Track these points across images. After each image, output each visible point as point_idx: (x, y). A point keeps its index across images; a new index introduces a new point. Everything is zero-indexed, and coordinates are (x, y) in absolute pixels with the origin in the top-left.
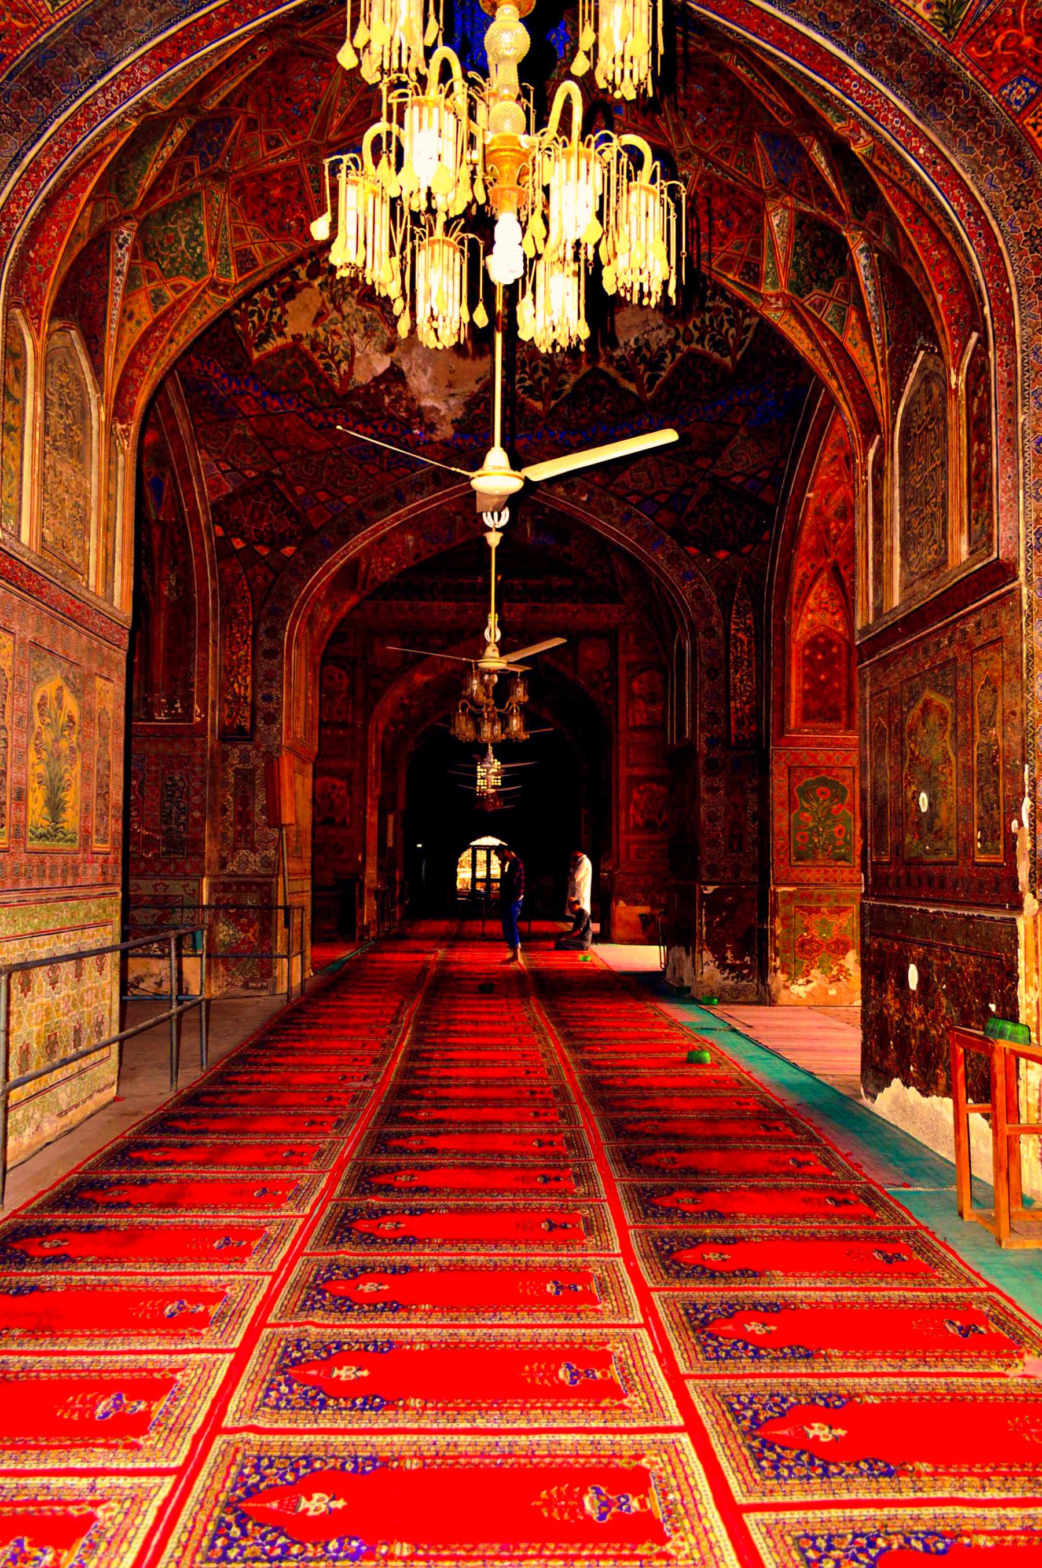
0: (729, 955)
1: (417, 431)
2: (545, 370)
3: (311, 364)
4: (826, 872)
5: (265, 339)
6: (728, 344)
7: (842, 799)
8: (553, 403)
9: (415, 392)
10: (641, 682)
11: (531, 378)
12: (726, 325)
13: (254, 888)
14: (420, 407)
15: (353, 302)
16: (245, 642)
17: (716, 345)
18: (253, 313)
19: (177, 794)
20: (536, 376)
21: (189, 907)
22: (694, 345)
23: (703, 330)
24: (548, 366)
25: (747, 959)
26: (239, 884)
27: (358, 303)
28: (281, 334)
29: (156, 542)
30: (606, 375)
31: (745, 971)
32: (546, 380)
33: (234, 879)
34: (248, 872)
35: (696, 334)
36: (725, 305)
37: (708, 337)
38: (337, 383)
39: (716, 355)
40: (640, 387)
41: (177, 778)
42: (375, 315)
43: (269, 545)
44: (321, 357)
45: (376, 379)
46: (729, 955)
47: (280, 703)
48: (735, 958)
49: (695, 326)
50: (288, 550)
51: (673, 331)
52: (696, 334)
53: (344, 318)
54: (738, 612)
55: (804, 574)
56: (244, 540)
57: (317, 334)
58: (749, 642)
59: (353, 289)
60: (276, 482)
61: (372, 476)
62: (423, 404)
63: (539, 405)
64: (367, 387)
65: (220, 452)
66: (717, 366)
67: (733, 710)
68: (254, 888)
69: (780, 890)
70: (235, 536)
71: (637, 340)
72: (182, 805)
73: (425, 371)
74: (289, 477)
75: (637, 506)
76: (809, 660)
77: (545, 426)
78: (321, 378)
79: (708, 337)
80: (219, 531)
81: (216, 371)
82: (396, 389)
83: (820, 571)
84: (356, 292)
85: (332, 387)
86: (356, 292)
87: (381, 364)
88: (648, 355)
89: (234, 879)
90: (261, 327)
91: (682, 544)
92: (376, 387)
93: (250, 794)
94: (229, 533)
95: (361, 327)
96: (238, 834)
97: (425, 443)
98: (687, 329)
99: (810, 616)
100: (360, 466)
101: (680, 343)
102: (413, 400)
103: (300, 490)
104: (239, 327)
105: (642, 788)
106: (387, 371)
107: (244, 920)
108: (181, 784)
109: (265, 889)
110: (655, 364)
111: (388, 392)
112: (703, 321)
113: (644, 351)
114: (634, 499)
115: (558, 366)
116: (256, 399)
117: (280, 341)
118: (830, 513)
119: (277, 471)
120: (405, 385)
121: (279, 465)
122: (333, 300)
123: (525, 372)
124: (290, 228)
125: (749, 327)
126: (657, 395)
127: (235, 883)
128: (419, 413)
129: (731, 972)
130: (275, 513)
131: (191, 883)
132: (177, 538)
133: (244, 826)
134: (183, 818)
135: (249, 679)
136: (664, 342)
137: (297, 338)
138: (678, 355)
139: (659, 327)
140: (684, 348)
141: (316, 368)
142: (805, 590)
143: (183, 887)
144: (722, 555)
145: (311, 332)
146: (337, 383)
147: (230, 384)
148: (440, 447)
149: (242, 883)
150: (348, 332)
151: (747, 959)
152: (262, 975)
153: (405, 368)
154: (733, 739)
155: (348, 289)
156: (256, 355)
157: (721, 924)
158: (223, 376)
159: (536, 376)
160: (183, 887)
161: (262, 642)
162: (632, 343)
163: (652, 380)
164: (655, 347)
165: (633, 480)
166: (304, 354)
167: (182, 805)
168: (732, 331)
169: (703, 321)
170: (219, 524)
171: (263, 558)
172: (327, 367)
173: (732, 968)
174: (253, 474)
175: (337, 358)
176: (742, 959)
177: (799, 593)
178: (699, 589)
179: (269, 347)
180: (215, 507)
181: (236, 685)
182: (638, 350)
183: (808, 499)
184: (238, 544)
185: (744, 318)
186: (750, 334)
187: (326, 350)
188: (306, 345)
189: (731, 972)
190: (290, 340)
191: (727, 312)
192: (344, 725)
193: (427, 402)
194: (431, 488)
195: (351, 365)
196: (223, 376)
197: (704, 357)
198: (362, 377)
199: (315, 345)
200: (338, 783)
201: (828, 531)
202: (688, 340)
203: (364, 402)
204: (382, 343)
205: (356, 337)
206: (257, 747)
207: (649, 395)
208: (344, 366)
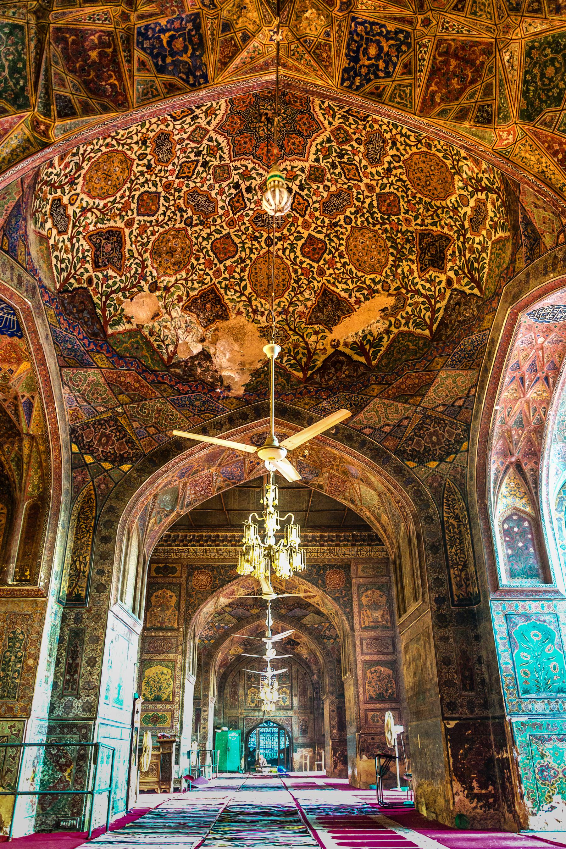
0: (475, 784)
1: (219, 390)
2: (303, 354)
3: (148, 344)
4: (549, 703)
5: (118, 323)
6: (426, 322)
7: (552, 641)
8: (310, 373)
9: (218, 367)
10: (367, 596)
11: (295, 358)
12: (424, 311)
13: (75, 730)
14: (221, 376)
15: (179, 310)
16: (88, 531)
17: (417, 325)
18: (110, 305)
19: (18, 645)
20: (298, 358)
21: (12, 746)
22: (402, 328)
23: (408, 319)
24: (306, 351)
25: (491, 788)
26: (62, 727)
27: (182, 311)
28: (129, 322)
29: (26, 451)
30: (344, 354)
31: (491, 800)
32: (305, 360)
33: (59, 723)
34: (71, 716)
35: (403, 321)
36: (421, 299)
37: (411, 321)
38: (165, 357)
39: (419, 331)
40: (367, 358)
41: (18, 632)
42: (193, 320)
43: (112, 462)
44: (156, 340)
45: (191, 357)
46: (475, 784)
47: (110, 576)
48: (481, 787)
49: (402, 317)
50: (126, 467)
51: (387, 322)
52: (403, 321)
53: (172, 319)
54: (449, 505)
55: (496, 469)
56: (95, 458)
57: (153, 326)
58: (459, 526)
59: (179, 302)
60: (119, 418)
61: (187, 418)
62: (223, 374)
63: (300, 375)
64: (186, 362)
65: (79, 391)
66: (420, 337)
67: (453, 576)
68: (75, 730)
69: (514, 720)
70: (86, 454)
71: (363, 331)
72: (19, 654)
73: (225, 355)
74: (129, 413)
75: (369, 436)
76: (507, 533)
77: (305, 387)
78: (155, 353)
79: (411, 321)
80: (75, 448)
81: (79, 333)
82: (205, 364)
83: (508, 468)
84: (181, 304)
85: (162, 359)
86: (181, 304)
87: (196, 349)
88: (371, 339)
89: (59, 723)
90: (115, 315)
91: (403, 460)
92: (192, 362)
93: (79, 648)
94: (83, 451)
95: (184, 326)
96: (67, 682)
97: (224, 398)
98: (396, 319)
99: (504, 500)
100: (179, 411)
101: (392, 328)
102: (216, 371)
103: (136, 424)
104: (99, 311)
105: (373, 669)
106: (200, 353)
107: (63, 760)
108: (21, 637)
109: (84, 731)
110: (376, 343)
111: (200, 365)
112: (407, 313)
113: (369, 337)
114: (367, 431)
115: (312, 351)
116: (107, 358)
117: (127, 326)
118: (511, 422)
119: (119, 409)
120: (211, 362)
121: (121, 405)
122: (165, 307)
123: (290, 355)
124: (105, 91)
125: (440, 308)
126: (380, 361)
127: (59, 726)
128: (221, 379)
129: (479, 801)
130: (118, 440)
131: (17, 724)
132: (42, 448)
133: (73, 675)
134: (19, 665)
135: (88, 558)
136: (382, 329)
137: (140, 327)
138: (392, 336)
139: (378, 321)
140: (396, 331)
141: (152, 346)
142: (499, 482)
143: (10, 727)
144: (433, 464)
145: (150, 324)
146: (165, 357)
147: (89, 345)
148: (234, 400)
149: (67, 726)
150: (175, 328)
151: (491, 788)
152: (73, 814)
153: (212, 351)
154: (456, 598)
155: (176, 302)
156: (110, 331)
157: (465, 756)
158: (84, 338)
159: (298, 358)
160: (10, 727)
161: (100, 531)
162: (360, 333)
163: (375, 354)
164: (375, 334)
165: (366, 419)
166: (143, 337)
167: (19, 654)
168: (429, 314)
169: (407, 313)
170: (75, 443)
171: (106, 471)
172: (159, 347)
173: (480, 797)
174: (103, 409)
175: (166, 342)
176: (487, 788)
177: (495, 483)
178: (418, 490)
179: (120, 328)
180: (73, 431)
181: (78, 563)
182: (365, 336)
183: (496, 411)
184: (89, 459)
185: (435, 304)
186: (441, 313)
187: (159, 336)
188: (146, 332)
189: (479, 801)
190: (135, 327)
191: (423, 303)
192: (172, 629)
193: (225, 373)
194: (228, 426)
195: (176, 347)
196: (84, 338)
197: (411, 334)
198: (182, 356)
199: (151, 333)
200: (165, 670)
201: (510, 437)
202: (398, 325)
203: (184, 371)
204: (197, 336)
205: (180, 331)
206: (89, 611)
207: (374, 363)
208: (171, 348)
